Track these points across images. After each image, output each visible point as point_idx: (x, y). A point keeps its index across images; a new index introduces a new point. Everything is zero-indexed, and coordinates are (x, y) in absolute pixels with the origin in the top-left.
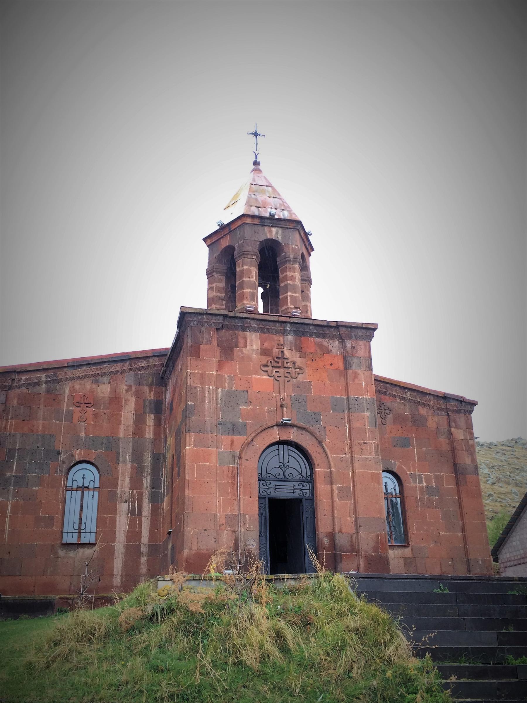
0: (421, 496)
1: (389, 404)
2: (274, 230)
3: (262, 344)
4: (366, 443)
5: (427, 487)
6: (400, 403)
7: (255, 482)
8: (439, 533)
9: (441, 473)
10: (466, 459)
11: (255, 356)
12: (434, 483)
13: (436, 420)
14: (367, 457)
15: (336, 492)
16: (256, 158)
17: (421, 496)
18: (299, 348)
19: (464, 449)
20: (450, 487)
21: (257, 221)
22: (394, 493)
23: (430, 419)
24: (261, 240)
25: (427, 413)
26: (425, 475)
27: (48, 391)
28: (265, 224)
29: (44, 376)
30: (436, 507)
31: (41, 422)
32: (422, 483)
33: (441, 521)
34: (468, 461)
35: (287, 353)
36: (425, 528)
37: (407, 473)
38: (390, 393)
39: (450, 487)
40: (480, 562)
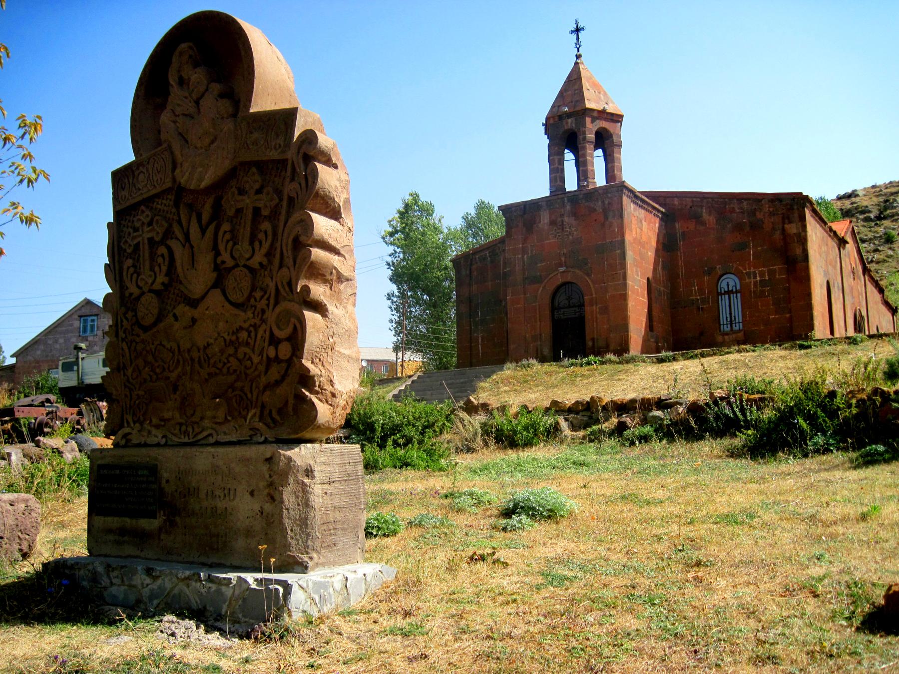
2: (569, 120)
3: (550, 218)
5: (760, 281)
7: (547, 312)
11: (546, 227)
16: (578, 51)
18: (575, 214)
22: (734, 290)
25: (764, 215)
26: (759, 271)
27: (492, 262)
29: (487, 252)
30: (768, 296)
31: (490, 283)
34: (799, 251)
35: (566, 219)
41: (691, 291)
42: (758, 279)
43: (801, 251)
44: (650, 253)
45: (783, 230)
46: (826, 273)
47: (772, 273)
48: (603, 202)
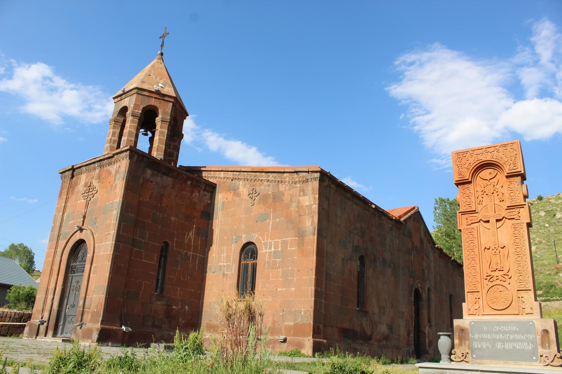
0: (269, 260)
1: (258, 189)
2: (126, 99)
4: (109, 234)
5: (274, 252)
6: (266, 185)
8: (277, 289)
9: (287, 238)
10: (307, 222)
12: (280, 248)
14: (108, 243)
15: (92, 269)
17: (269, 260)
18: (99, 177)
19: (307, 214)
20: (292, 249)
21: (119, 99)
23: (286, 194)
24: (119, 110)
25: (285, 188)
28: (122, 98)
32: (271, 249)
33: (280, 279)
36: (267, 285)
37: (262, 242)
38: (258, 179)
39: (292, 249)
40: (303, 313)
41: (220, 257)
42: (273, 249)
43: (310, 223)
44: (173, 219)
46: (356, 249)
47: (284, 244)
48: (117, 166)
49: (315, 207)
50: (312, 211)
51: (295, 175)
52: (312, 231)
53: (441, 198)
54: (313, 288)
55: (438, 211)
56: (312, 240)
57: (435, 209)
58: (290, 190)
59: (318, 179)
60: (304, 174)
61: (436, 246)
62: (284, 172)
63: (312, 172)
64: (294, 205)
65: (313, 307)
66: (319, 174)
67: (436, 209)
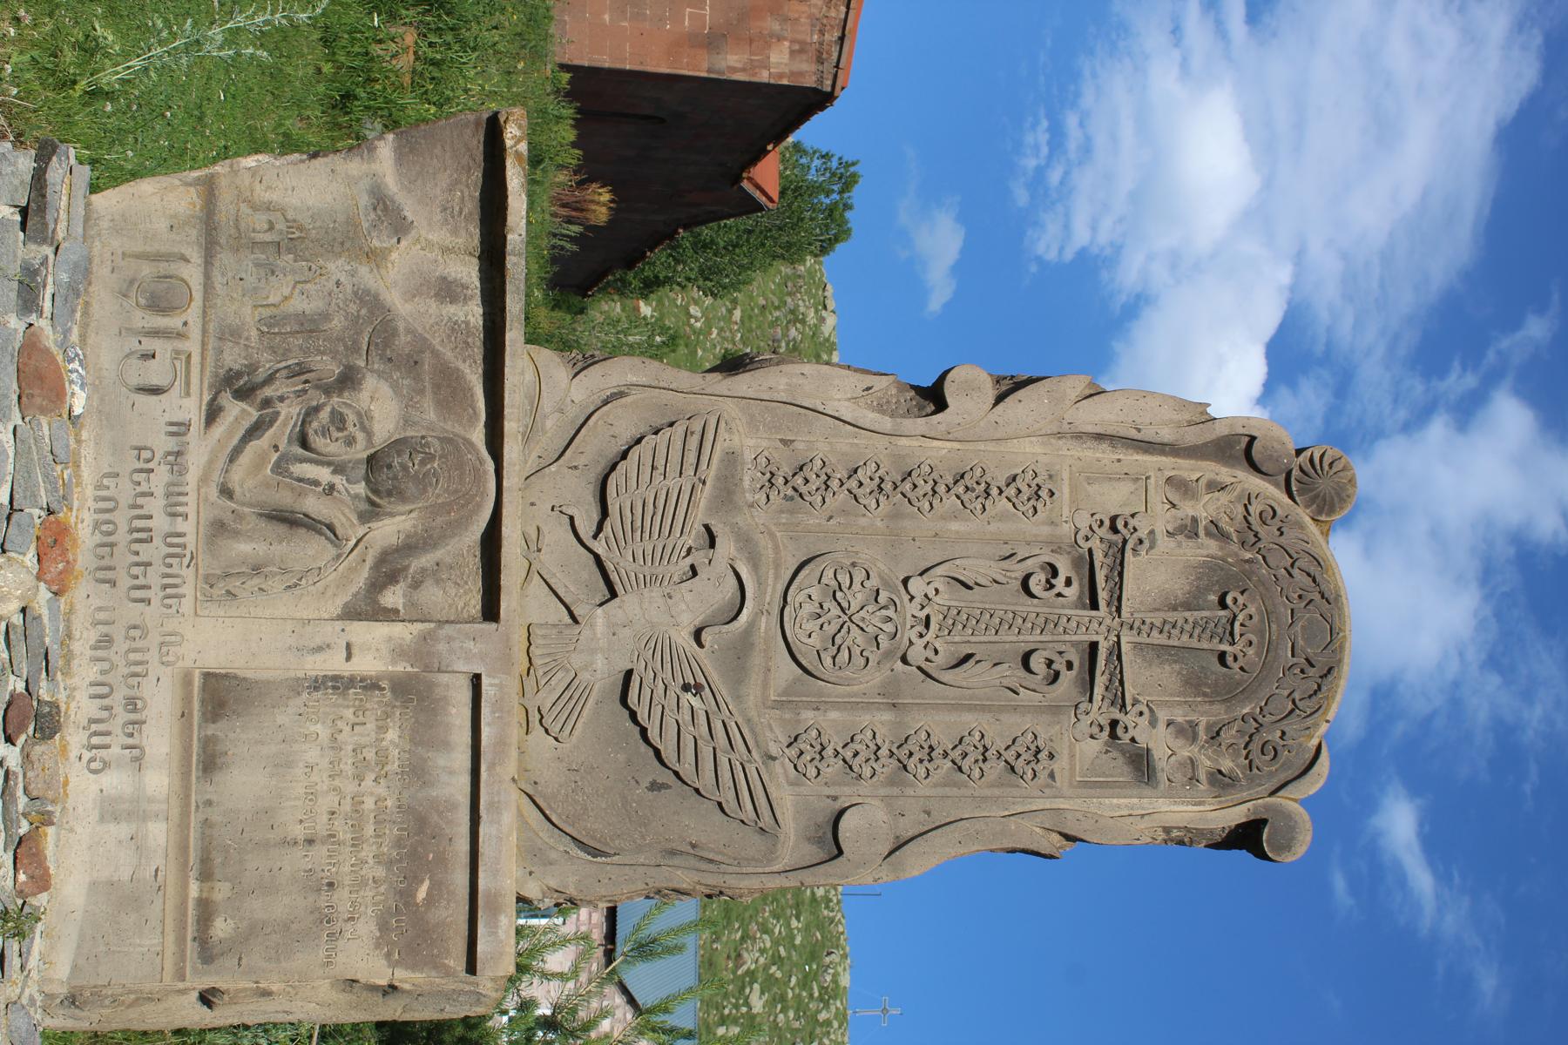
10: (735, 57)
13: (802, 20)
45: (780, 39)
49: (764, 77)
50: (757, 70)
51: (837, 34)
52: (717, 67)
53: (856, 182)
54: (607, 65)
55: (817, 163)
56: (697, 66)
57: (826, 157)
58: (808, 17)
59: (820, 87)
60: (835, 55)
61: (681, 231)
62: (848, 7)
63: (835, 76)
64: (776, 27)
65: (570, 63)
66: (829, 89)
67: (823, 157)
